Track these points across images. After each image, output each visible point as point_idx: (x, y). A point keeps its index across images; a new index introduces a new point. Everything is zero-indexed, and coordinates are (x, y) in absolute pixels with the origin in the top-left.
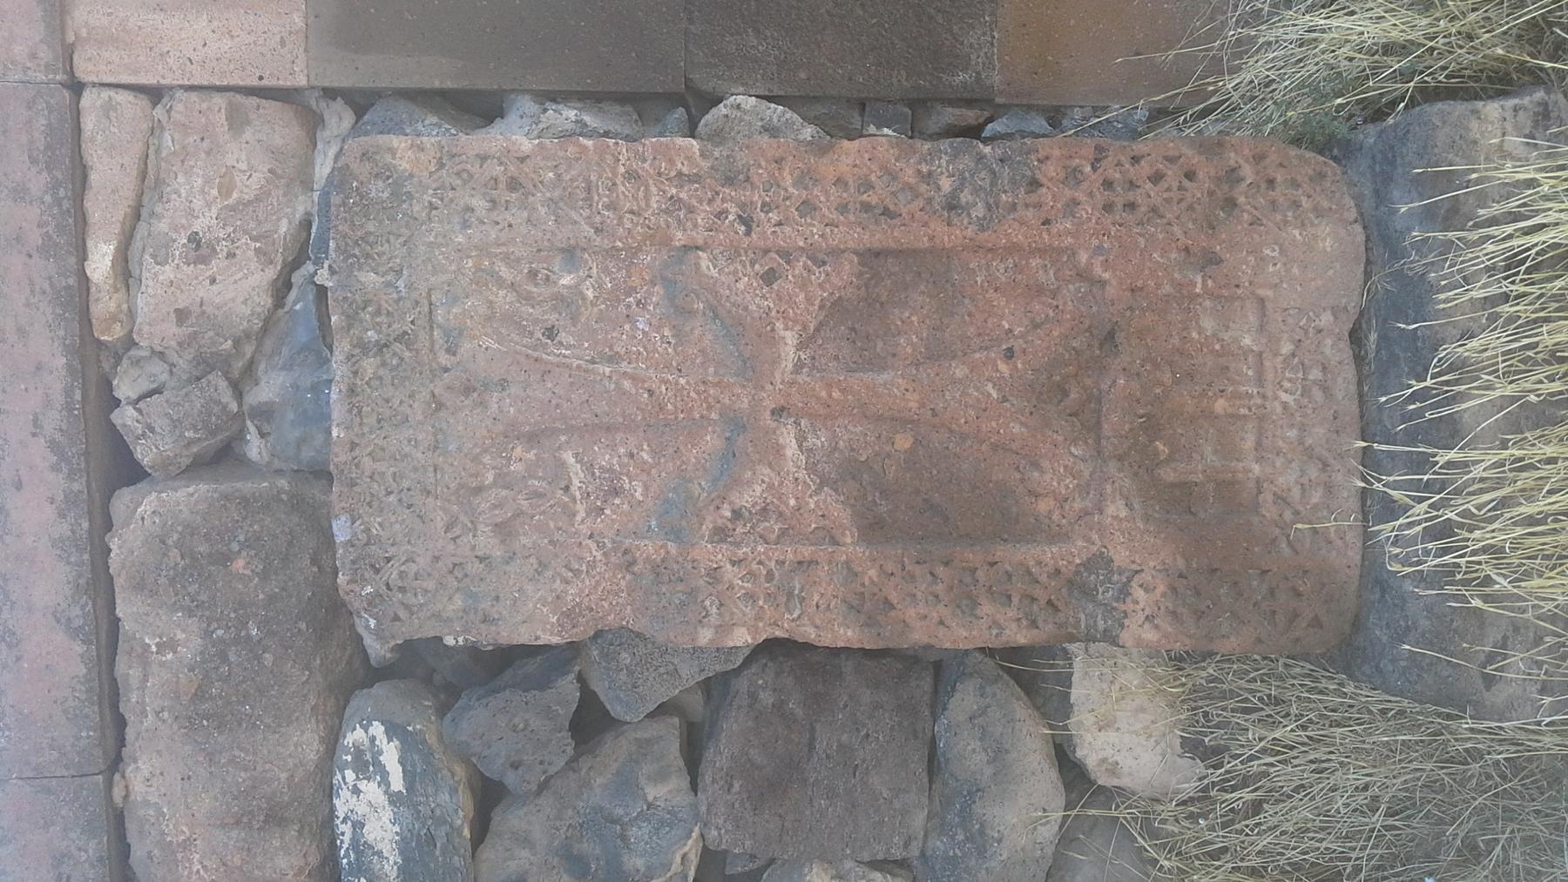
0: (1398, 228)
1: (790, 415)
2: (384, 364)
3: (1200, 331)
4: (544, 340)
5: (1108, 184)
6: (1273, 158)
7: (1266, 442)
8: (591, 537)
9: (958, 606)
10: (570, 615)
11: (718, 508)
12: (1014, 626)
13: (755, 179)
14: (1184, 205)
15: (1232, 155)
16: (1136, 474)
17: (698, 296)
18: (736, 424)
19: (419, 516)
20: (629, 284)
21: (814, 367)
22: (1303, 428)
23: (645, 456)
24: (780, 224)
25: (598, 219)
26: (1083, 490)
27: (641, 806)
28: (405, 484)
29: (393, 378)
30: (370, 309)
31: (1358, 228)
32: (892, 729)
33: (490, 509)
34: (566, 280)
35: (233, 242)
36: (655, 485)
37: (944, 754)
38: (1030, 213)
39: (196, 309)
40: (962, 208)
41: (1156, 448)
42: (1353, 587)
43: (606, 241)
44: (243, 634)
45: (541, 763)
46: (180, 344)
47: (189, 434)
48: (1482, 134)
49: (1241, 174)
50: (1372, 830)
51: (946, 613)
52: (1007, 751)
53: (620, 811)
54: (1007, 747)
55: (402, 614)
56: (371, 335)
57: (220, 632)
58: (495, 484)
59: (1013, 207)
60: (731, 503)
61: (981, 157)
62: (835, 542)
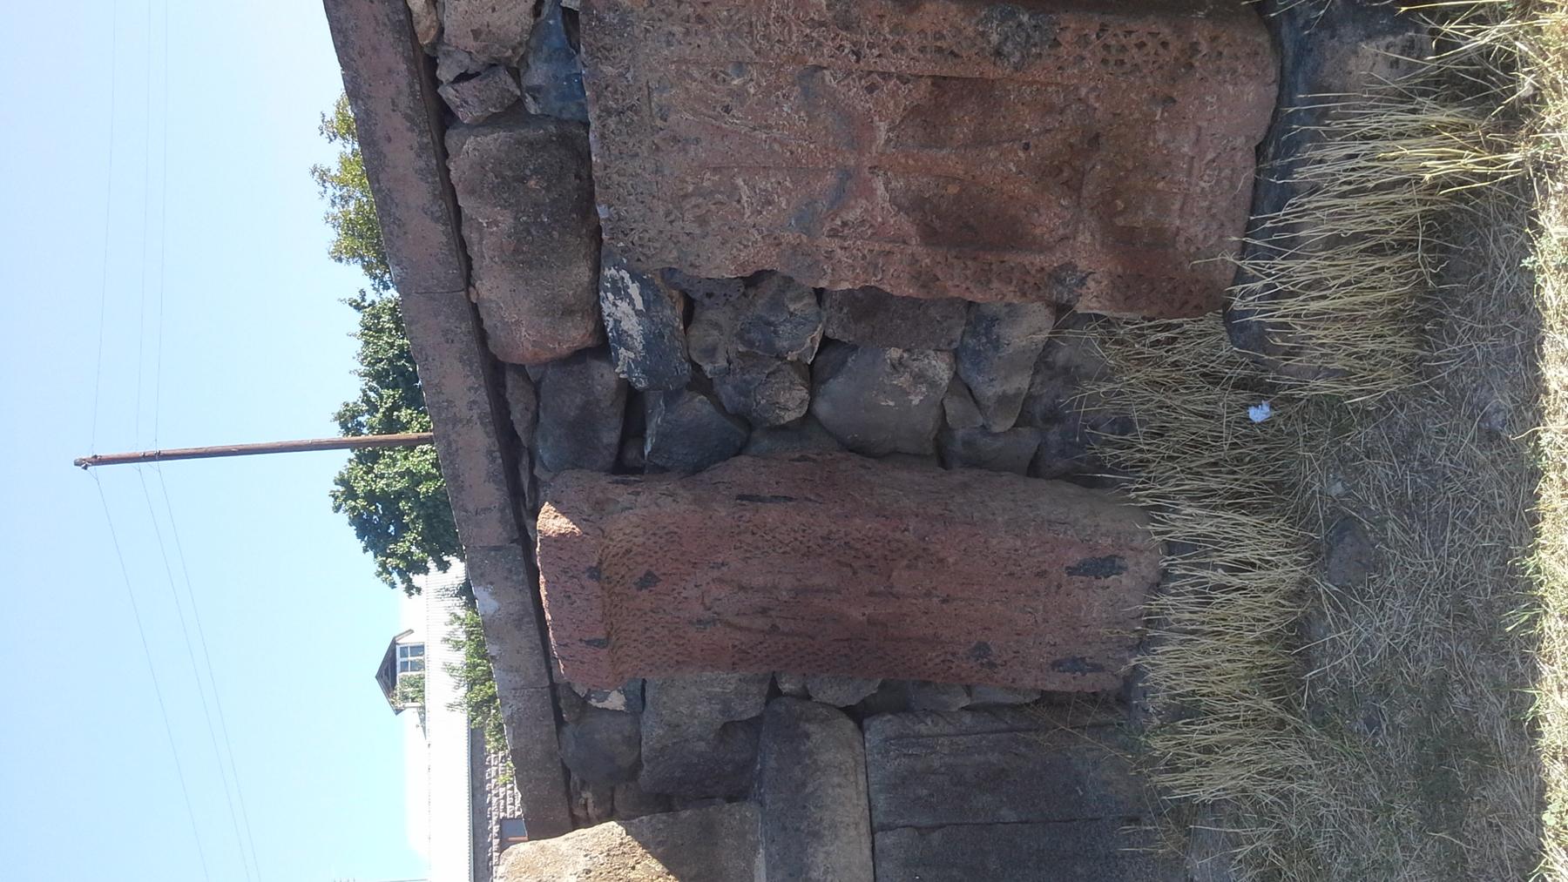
3: (1155, 141)
8: (754, 226)
14: (1156, 65)
15: (1196, 34)
18: (846, 174)
20: (778, 83)
24: (879, 56)
25: (757, 46)
28: (639, 190)
30: (610, 89)
41: (1116, 205)
48: (1357, 67)
51: (972, 286)
53: (773, 319)
55: (641, 258)
57: (524, 218)
59: (1040, 55)
60: (841, 217)
61: (1020, 25)
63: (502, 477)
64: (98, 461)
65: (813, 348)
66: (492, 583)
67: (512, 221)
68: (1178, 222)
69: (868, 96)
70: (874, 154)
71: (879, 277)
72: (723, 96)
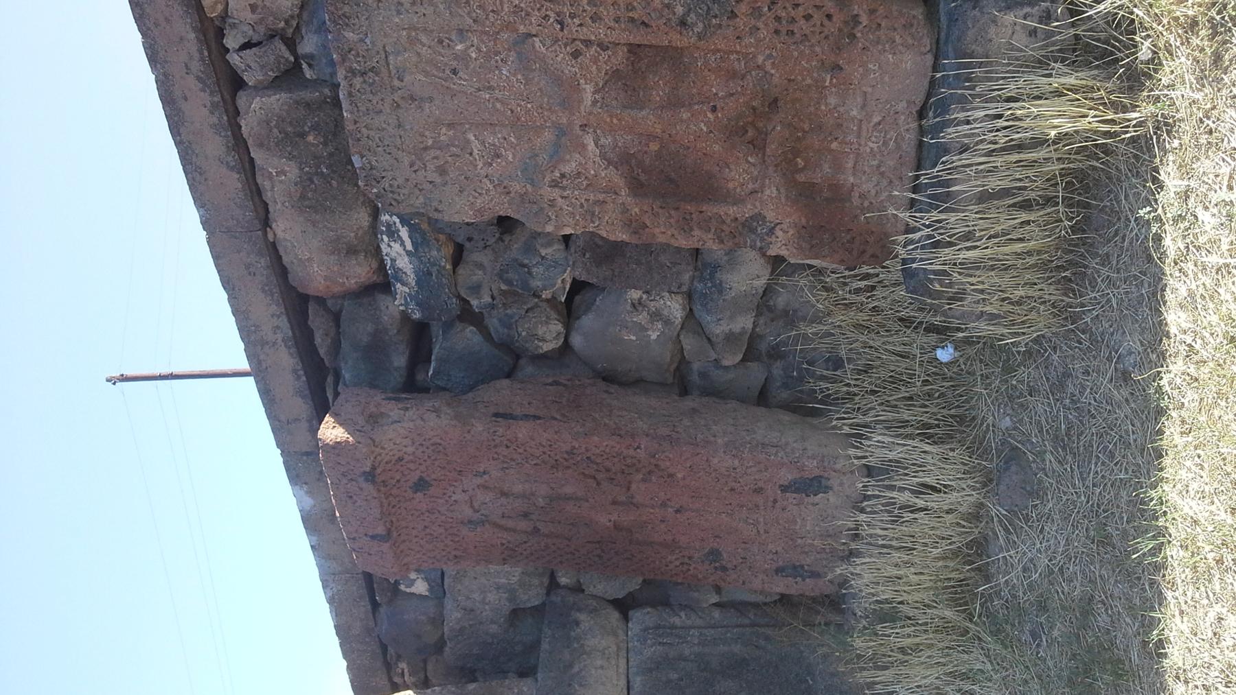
8: (486, 176)
12: (711, 241)
14: (822, 35)
15: (856, 7)
16: (784, 174)
18: (561, 132)
20: (496, 49)
24: (581, 25)
30: (353, 52)
40: (689, 26)
48: (997, 35)
51: (676, 233)
53: (526, 261)
55: (393, 203)
59: (720, 26)
60: (559, 170)
63: (307, 392)
64: (125, 379)
65: (565, 288)
66: (306, 483)
67: (297, 171)
68: (851, 179)
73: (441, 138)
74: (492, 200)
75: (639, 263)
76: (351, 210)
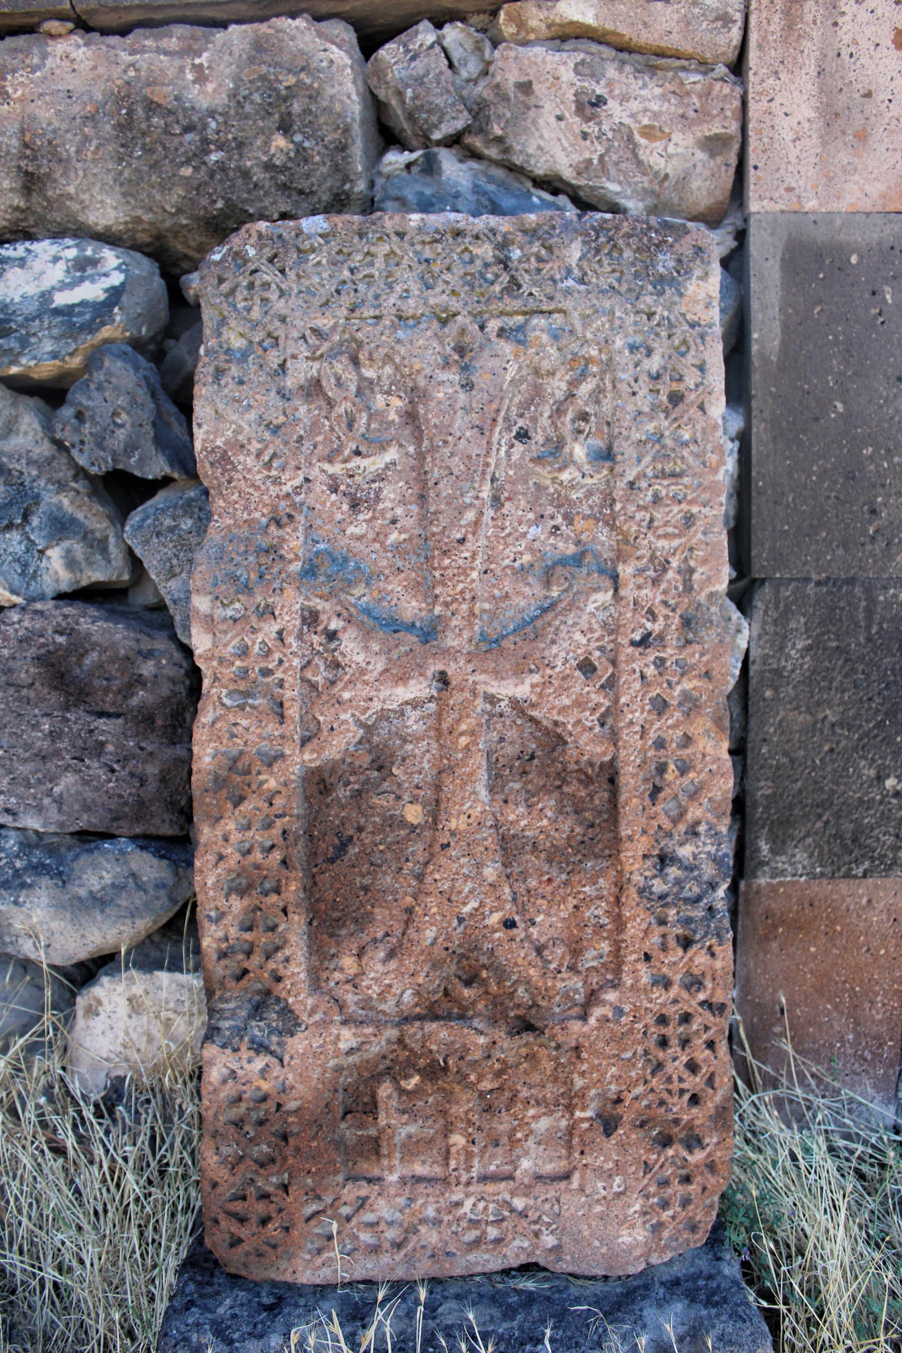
0: (645, 1313)
1: (440, 690)
2: (486, 265)
4: (515, 429)
5: (686, 1018)
6: (712, 1180)
7: (421, 1188)
8: (307, 480)
9: (239, 875)
10: (223, 460)
11: (339, 615)
12: (220, 934)
13: (689, 650)
14: (665, 1095)
15: (715, 1140)
16: (384, 1057)
17: (566, 591)
19: (327, 303)
20: (577, 519)
21: (491, 715)
22: (437, 1222)
23: (394, 537)
24: (643, 677)
25: (643, 484)
26: (366, 1004)
27: (41, 544)
28: (362, 287)
29: (472, 274)
30: (543, 252)
31: (641, 1266)
32: (120, 796)
33: (335, 374)
34: (579, 451)
35: (598, 138)
36: (362, 547)
37: (97, 848)
38: (656, 939)
39: (532, 101)
40: (662, 870)
41: (412, 1076)
42: (273, 1275)
43: (621, 493)
44: (212, 147)
45: (82, 442)
46: (498, 86)
47: (409, 93)
49: (696, 1151)
50: (40, 1269)
52: (102, 911)
53: (35, 521)
54: (107, 911)
55: (225, 287)
56: (516, 254)
58: (362, 378)
59: (662, 922)
61: (713, 886)
62: (305, 741)
67: (205, 106)
69: (574, 663)
70: (471, 679)
71: (228, 702)
72: (544, 430)
73: (379, 396)
74: (257, 488)
75: (54, 735)
76: (124, 195)
